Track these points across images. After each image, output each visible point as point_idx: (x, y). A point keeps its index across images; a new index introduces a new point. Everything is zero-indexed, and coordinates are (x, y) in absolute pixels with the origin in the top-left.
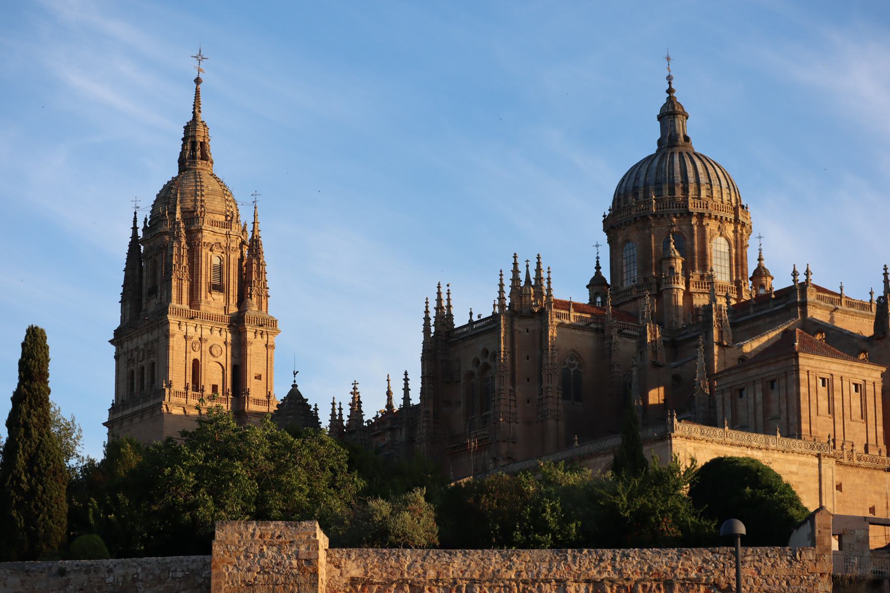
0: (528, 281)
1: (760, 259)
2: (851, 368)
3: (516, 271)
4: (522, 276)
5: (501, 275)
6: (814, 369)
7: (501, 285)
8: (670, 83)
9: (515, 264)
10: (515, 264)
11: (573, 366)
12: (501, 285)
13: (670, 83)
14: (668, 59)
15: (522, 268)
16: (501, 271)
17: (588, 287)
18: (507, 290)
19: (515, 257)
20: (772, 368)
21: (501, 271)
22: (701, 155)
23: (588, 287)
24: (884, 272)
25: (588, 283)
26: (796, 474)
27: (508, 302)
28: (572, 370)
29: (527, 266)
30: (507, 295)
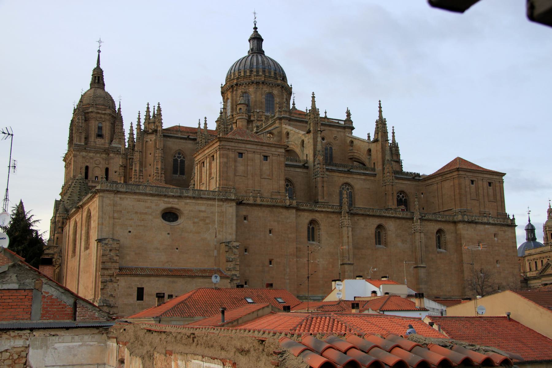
0: (154, 116)
1: (294, 104)
2: (262, 147)
3: (148, 111)
4: (151, 114)
5: (139, 114)
6: (233, 148)
7: (139, 119)
8: (255, 26)
9: (148, 108)
10: (148, 108)
11: (180, 157)
12: (139, 119)
13: (255, 26)
14: (255, 13)
15: (151, 110)
16: (139, 112)
17: (216, 122)
18: (143, 121)
19: (148, 105)
20: (210, 149)
21: (139, 112)
22: (269, 58)
23: (216, 122)
24: (312, 96)
25: (216, 120)
26: (205, 212)
27: (143, 127)
28: (179, 160)
29: (154, 109)
30: (142, 124)
